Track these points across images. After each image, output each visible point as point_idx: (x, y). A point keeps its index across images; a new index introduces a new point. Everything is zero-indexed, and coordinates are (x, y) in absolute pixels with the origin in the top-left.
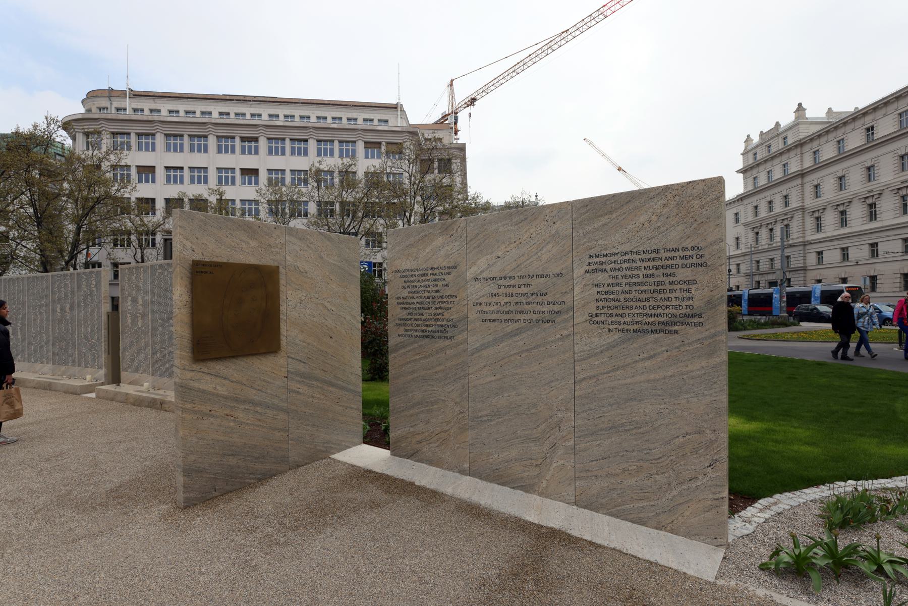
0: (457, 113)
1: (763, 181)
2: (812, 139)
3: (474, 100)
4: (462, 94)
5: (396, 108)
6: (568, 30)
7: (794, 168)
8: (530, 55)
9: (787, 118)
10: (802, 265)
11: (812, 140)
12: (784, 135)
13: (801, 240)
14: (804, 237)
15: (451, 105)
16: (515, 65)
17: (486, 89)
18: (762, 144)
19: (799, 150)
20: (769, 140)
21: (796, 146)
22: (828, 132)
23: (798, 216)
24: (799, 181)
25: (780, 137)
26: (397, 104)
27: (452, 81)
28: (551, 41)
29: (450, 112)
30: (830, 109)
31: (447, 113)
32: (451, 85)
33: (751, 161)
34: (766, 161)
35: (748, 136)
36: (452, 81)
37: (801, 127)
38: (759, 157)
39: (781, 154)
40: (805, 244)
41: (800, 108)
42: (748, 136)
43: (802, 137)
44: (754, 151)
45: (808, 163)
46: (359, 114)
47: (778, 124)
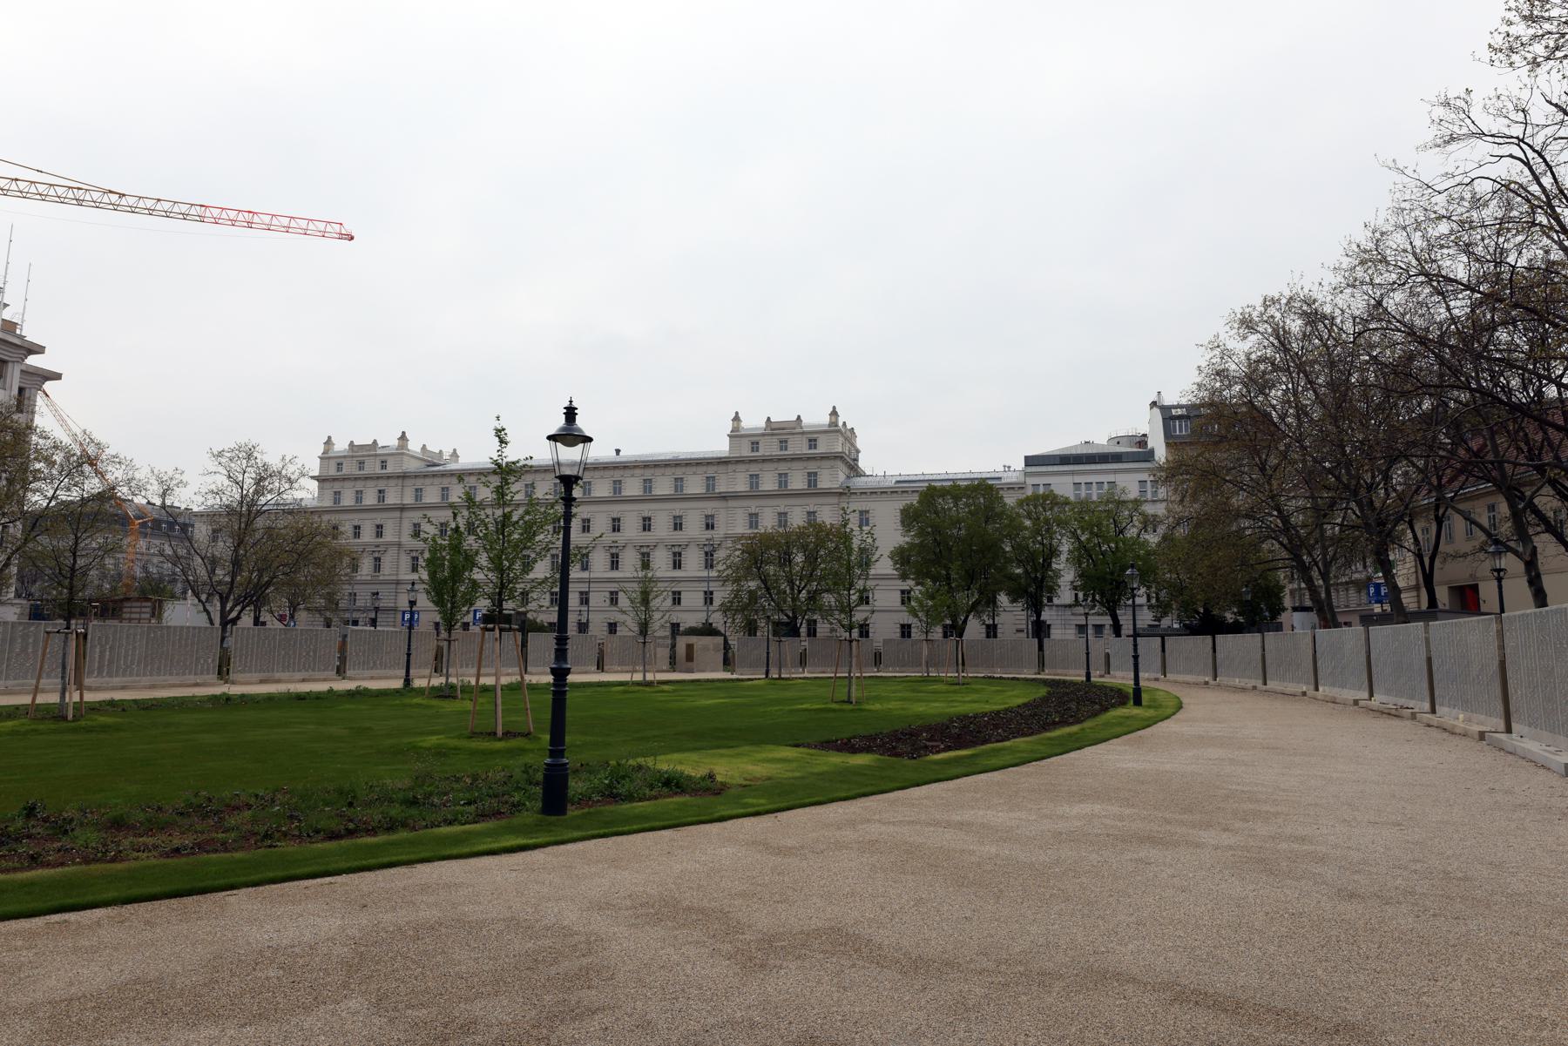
1: (348, 500)
2: (416, 476)
6: (124, 195)
7: (392, 499)
9: (389, 440)
10: (393, 605)
12: (383, 458)
13: (394, 578)
14: (397, 575)
19: (400, 481)
20: (363, 456)
21: (398, 477)
23: (392, 552)
24: (397, 514)
25: (378, 458)
30: (424, 445)
33: (333, 472)
35: (329, 438)
38: (345, 471)
40: (398, 583)
41: (403, 437)
42: (329, 438)
44: (339, 461)
45: (409, 499)
47: (375, 442)
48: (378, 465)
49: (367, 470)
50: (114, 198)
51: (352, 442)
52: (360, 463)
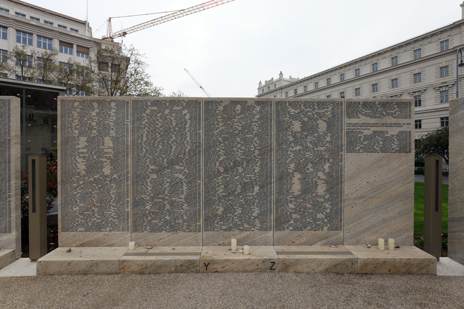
0: (113, 38)
3: (125, 34)
4: (117, 28)
5: (84, 24)
6: (184, 10)
8: (162, 17)
9: (276, 77)
11: (285, 87)
12: (275, 84)
15: (109, 32)
16: (153, 20)
17: (134, 29)
18: (266, 86)
19: (280, 91)
20: (269, 85)
21: (280, 89)
22: (291, 85)
26: (85, 21)
27: (110, 18)
28: (174, 13)
29: (109, 36)
30: (290, 76)
31: (106, 37)
32: (110, 21)
33: (261, 93)
34: (267, 93)
36: (110, 18)
37: (282, 81)
39: (274, 91)
41: (281, 74)
43: (282, 86)
46: (55, 20)
48: (274, 86)
49: (271, 89)
50: (182, 12)
51: (266, 81)
52: (269, 88)
